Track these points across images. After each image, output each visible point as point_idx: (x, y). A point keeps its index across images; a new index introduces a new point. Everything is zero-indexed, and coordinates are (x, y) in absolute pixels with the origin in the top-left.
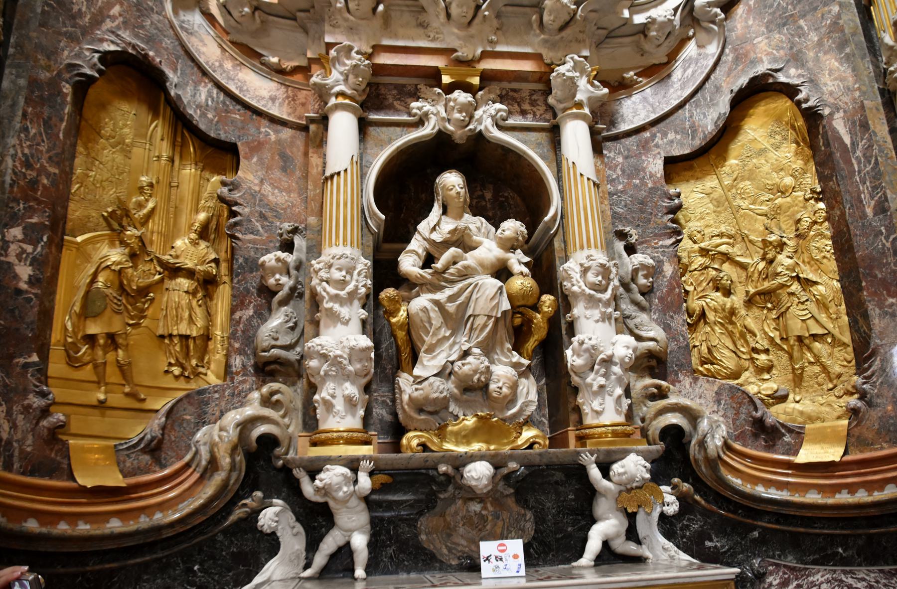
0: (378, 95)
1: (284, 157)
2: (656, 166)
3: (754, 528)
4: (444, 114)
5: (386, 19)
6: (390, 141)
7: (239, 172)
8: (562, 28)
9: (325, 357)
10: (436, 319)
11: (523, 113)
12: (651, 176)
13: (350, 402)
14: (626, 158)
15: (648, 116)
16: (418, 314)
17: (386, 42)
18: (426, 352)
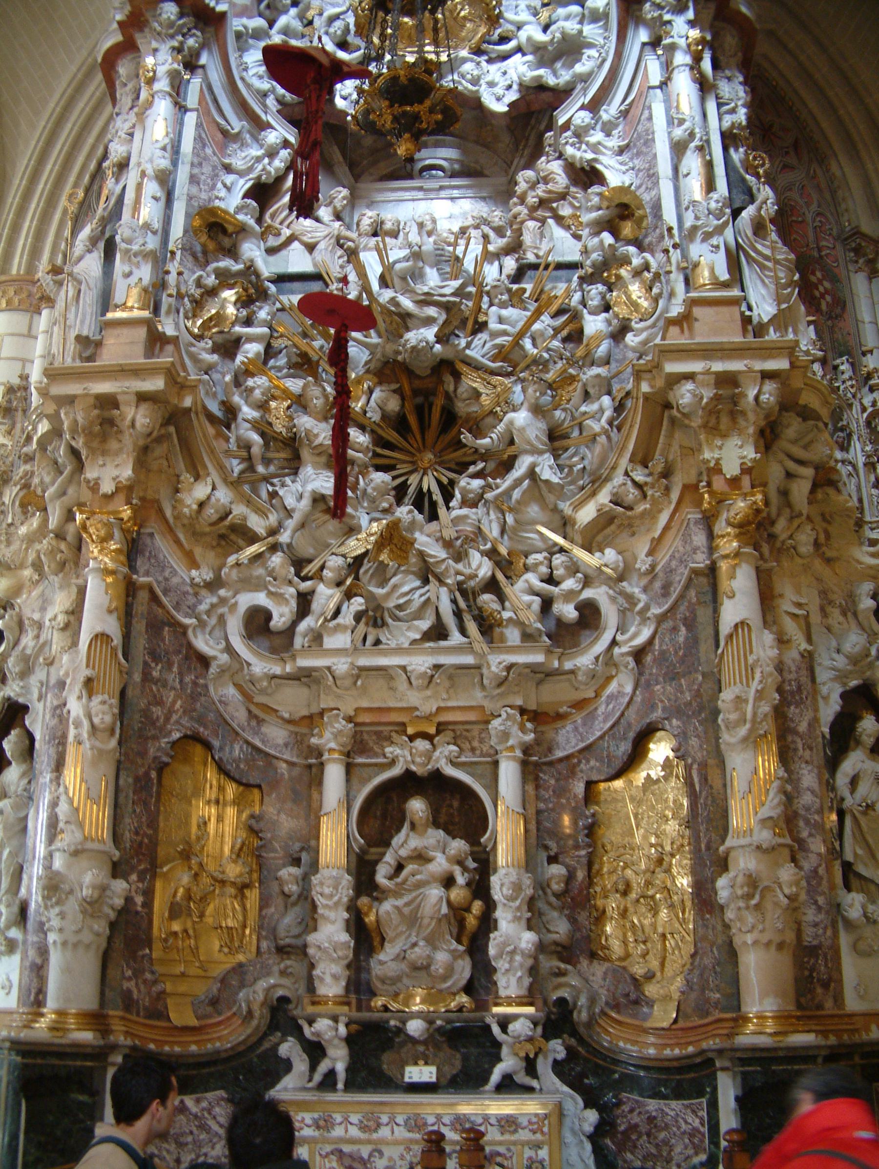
0: (362, 741)
1: (294, 791)
2: (579, 788)
3: (615, 1072)
4: (409, 758)
5: (364, 688)
6: (370, 779)
8: (499, 685)
9: (319, 947)
10: (395, 917)
11: (473, 750)
12: (575, 796)
13: (335, 977)
14: (557, 780)
17: (365, 704)
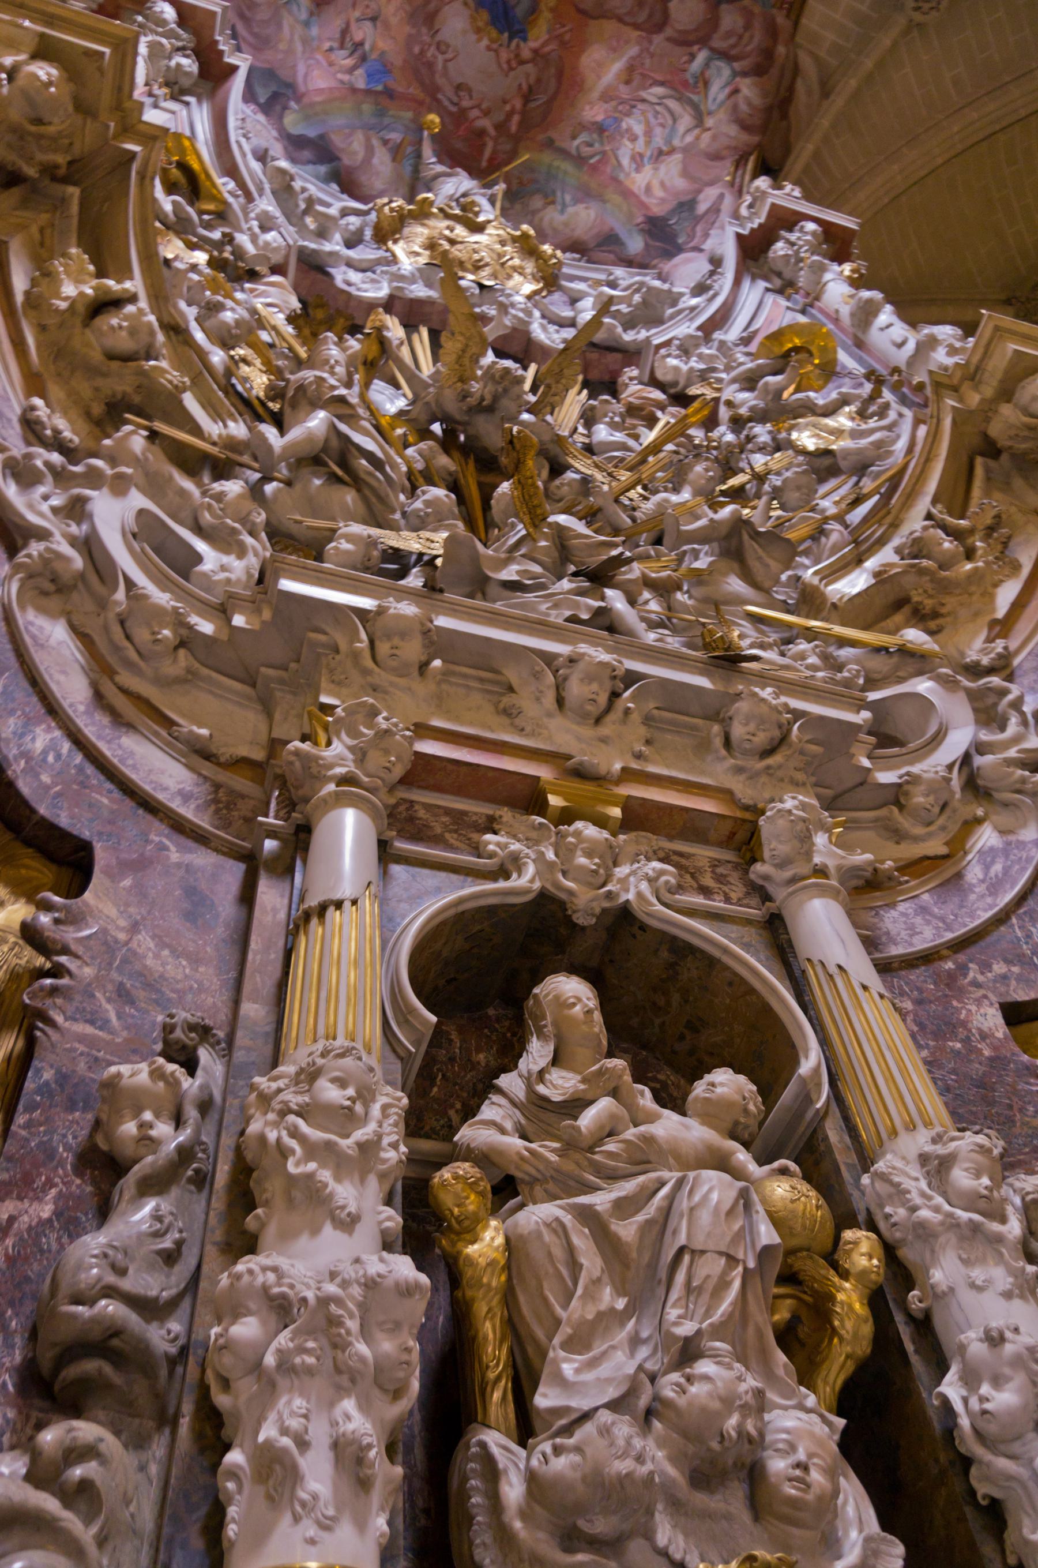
7: (87, 895)
8: (768, 752)
9: (282, 1309)
11: (705, 891)
12: (984, 1036)
14: (918, 1002)
15: (941, 936)
16: (539, 1235)
18: (571, 1345)
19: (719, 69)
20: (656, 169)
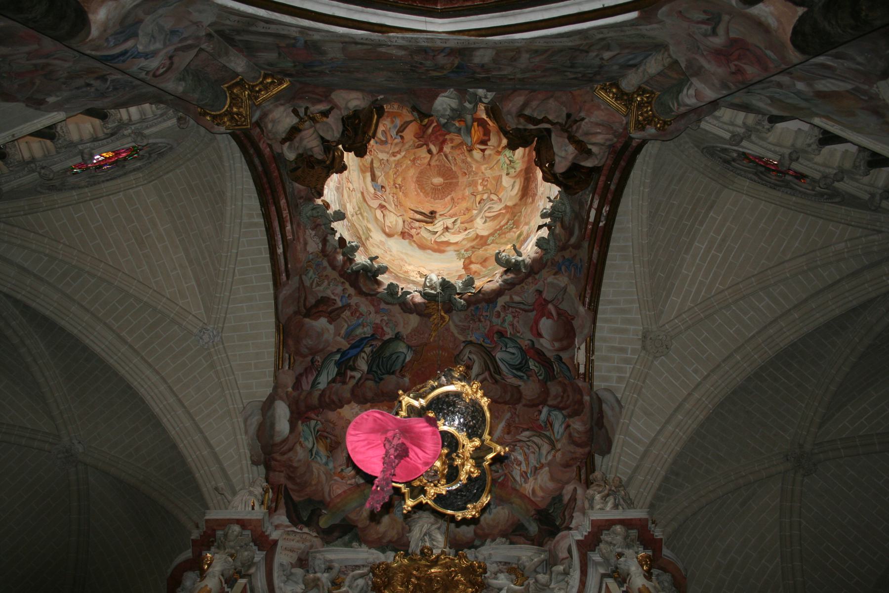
19: (556, 415)
20: (536, 479)
